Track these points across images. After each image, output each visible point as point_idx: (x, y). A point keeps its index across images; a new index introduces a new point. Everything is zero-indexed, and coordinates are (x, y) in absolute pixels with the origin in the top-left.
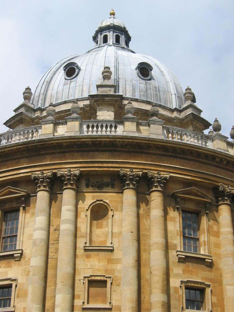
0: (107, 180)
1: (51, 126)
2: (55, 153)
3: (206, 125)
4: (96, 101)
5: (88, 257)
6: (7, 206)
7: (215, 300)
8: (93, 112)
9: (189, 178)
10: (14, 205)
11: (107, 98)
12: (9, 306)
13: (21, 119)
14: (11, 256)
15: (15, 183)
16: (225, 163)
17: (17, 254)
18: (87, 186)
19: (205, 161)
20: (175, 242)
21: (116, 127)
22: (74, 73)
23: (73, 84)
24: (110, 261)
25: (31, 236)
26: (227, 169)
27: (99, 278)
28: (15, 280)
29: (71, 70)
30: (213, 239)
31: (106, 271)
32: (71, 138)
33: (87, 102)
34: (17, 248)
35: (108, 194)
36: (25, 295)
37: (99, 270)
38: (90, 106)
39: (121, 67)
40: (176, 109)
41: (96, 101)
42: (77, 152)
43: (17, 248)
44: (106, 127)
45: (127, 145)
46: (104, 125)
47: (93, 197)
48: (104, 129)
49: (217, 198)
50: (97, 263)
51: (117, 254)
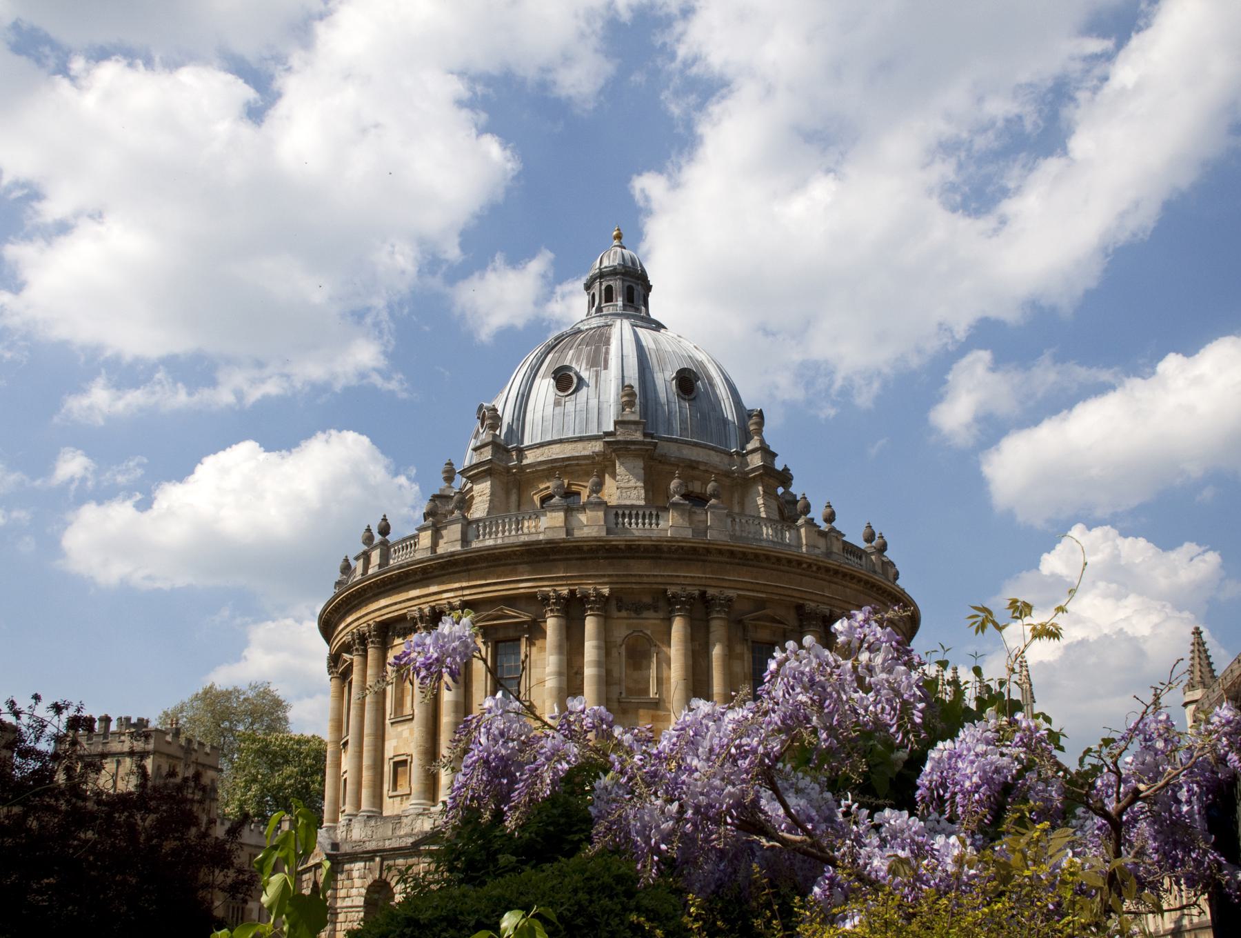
0: (647, 599)
1: (562, 514)
4: (614, 451)
6: (501, 635)
10: (512, 633)
15: (510, 601)
18: (619, 611)
21: (657, 516)
23: (570, 406)
32: (596, 539)
33: (598, 447)
38: (603, 454)
44: (644, 518)
45: (676, 550)
46: (641, 513)
49: (801, 620)
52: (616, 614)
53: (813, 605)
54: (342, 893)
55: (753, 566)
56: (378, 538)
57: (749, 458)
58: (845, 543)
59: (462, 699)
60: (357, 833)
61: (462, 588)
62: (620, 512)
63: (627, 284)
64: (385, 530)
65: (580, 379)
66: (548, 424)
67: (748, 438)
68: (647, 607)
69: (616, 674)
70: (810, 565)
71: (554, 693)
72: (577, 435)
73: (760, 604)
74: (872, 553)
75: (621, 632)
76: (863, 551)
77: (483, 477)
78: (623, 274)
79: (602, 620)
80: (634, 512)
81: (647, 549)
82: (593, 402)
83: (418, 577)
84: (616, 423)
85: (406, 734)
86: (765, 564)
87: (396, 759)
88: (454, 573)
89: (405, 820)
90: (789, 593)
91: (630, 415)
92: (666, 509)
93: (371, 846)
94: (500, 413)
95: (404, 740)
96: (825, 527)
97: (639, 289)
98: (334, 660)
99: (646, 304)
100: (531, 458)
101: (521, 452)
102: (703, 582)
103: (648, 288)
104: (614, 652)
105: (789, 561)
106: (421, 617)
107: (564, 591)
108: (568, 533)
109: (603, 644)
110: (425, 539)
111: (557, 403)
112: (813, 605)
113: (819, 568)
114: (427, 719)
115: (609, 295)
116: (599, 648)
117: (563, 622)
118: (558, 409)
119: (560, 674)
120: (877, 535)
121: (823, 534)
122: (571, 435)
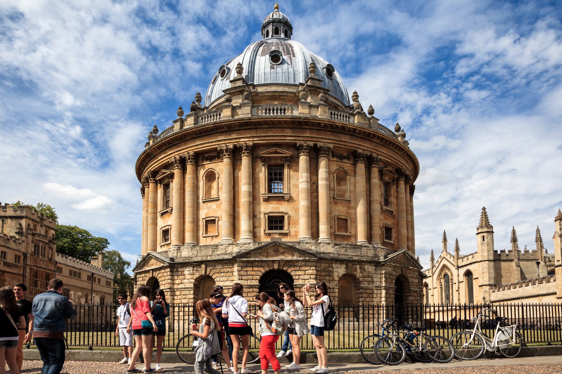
4: (310, 90)
5: (336, 203)
23: (279, 69)
24: (349, 208)
27: (343, 217)
31: (347, 213)
36: (297, 223)
37: (343, 212)
51: (353, 204)
63: (285, 28)
77: (237, 95)
87: (207, 219)
97: (289, 32)
111: (272, 68)
114: (230, 199)
115: (276, 32)
118: (272, 70)
122: (280, 82)
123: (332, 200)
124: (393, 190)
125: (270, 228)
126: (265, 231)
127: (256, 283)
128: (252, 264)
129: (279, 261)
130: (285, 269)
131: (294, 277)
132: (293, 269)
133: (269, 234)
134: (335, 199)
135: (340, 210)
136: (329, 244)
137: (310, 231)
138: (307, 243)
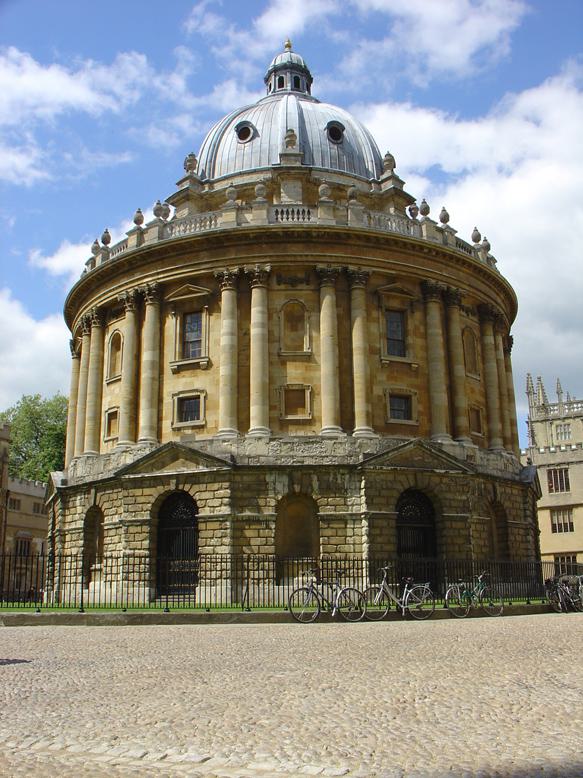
0: (301, 275)
2: (239, 245)
3: (410, 200)
6: (187, 308)
7: (420, 408)
8: (275, 186)
9: (393, 272)
10: (195, 306)
11: (292, 171)
12: (198, 419)
13: (188, 195)
14: (196, 366)
16: (434, 253)
17: (203, 362)
19: (412, 252)
20: (378, 346)
22: (248, 135)
25: (217, 342)
26: (435, 261)
28: (202, 391)
29: (244, 132)
30: (419, 342)
31: (304, 379)
32: (259, 228)
33: (269, 175)
34: (203, 355)
35: (304, 292)
36: (216, 407)
38: (272, 180)
39: (308, 127)
40: (374, 181)
41: (279, 175)
42: (266, 243)
43: (203, 355)
45: (323, 236)
46: (296, 210)
47: (286, 296)
48: (296, 216)
49: (424, 294)
50: (293, 371)
52: (277, 287)
53: (433, 281)
54: (69, 519)
55: (385, 249)
56: (101, 245)
57: (383, 186)
58: (457, 239)
59: (158, 360)
60: (80, 472)
61: (158, 274)
62: (280, 210)
64: (106, 240)
65: (256, 131)
66: (232, 164)
67: (381, 170)
68: (301, 281)
69: (276, 334)
70: (430, 250)
71: (227, 349)
72: (253, 168)
73: (392, 279)
74: (479, 250)
75: (280, 300)
76: (473, 248)
78: (291, 68)
79: (265, 291)
80: (290, 210)
81: (299, 234)
82: (265, 146)
83: (126, 269)
84: (281, 155)
85: (117, 391)
86: (395, 248)
87: (110, 411)
88: (152, 262)
89: (112, 457)
90: (415, 271)
91: (290, 150)
92: (315, 207)
93: (88, 480)
94: (198, 159)
95: (115, 397)
96: (440, 225)
97: (303, 81)
98: (74, 344)
99: (309, 90)
100: (218, 187)
101: (211, 184)
102: (345, 260)
103: (310, 80)
104: (275, 316)
105: (413, 246)
106: (128, 298)
107: (235, 270)
108: (238, 224)
109: (266, 311)
110: (133, 242)
112: (433, 281)
113: (437, 253)
115: (281, 84)
116: (263, 312)
117: (234, 293)
119: (232, 334)
120: (482, 239)
121: (440, 230)
123: (275, 359)
124: (414, 321)
125: (181, 419)
126: (172, 424)
127: (146, 516)
128: (139, 484)
129: (177, 477)
130: (187, 488)
131: (198, 502)
132: (196, 488)
133: (179, 429)
134: (276, 360)
135: (294, 374)
136: (260, 438)
137: (235, 419)
138: (224, 441)
